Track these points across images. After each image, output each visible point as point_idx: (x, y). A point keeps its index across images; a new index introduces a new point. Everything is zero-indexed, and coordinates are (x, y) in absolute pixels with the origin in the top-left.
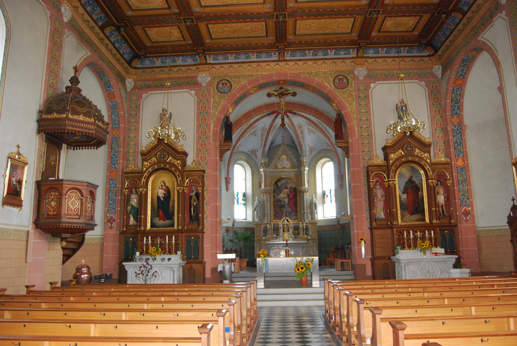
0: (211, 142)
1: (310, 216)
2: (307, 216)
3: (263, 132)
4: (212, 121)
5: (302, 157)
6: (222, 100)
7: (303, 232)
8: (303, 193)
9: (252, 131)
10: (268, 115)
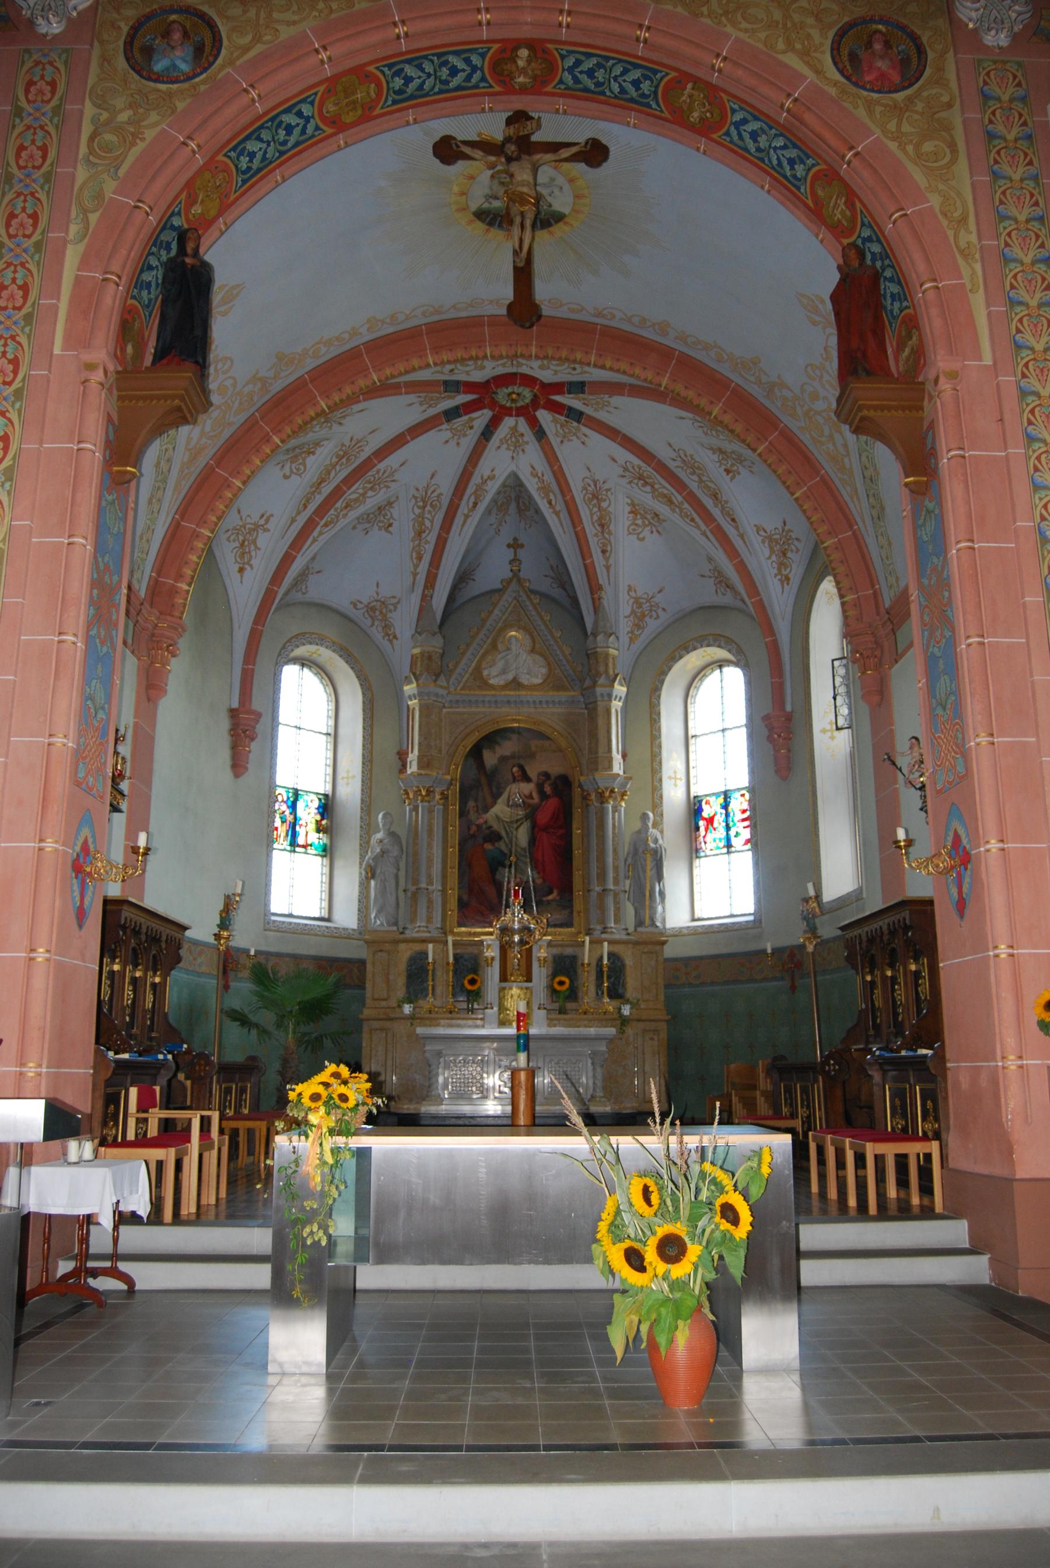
0: (57, 351)
1: (629, 910)
2: (617, 910)
3: (421, 516)
4: (74, 229)
5: (600, 638)
6: (154, 117)
7: (599, 985)
8: (602, 798)
9: (372, 502)
10: (451, 414)
